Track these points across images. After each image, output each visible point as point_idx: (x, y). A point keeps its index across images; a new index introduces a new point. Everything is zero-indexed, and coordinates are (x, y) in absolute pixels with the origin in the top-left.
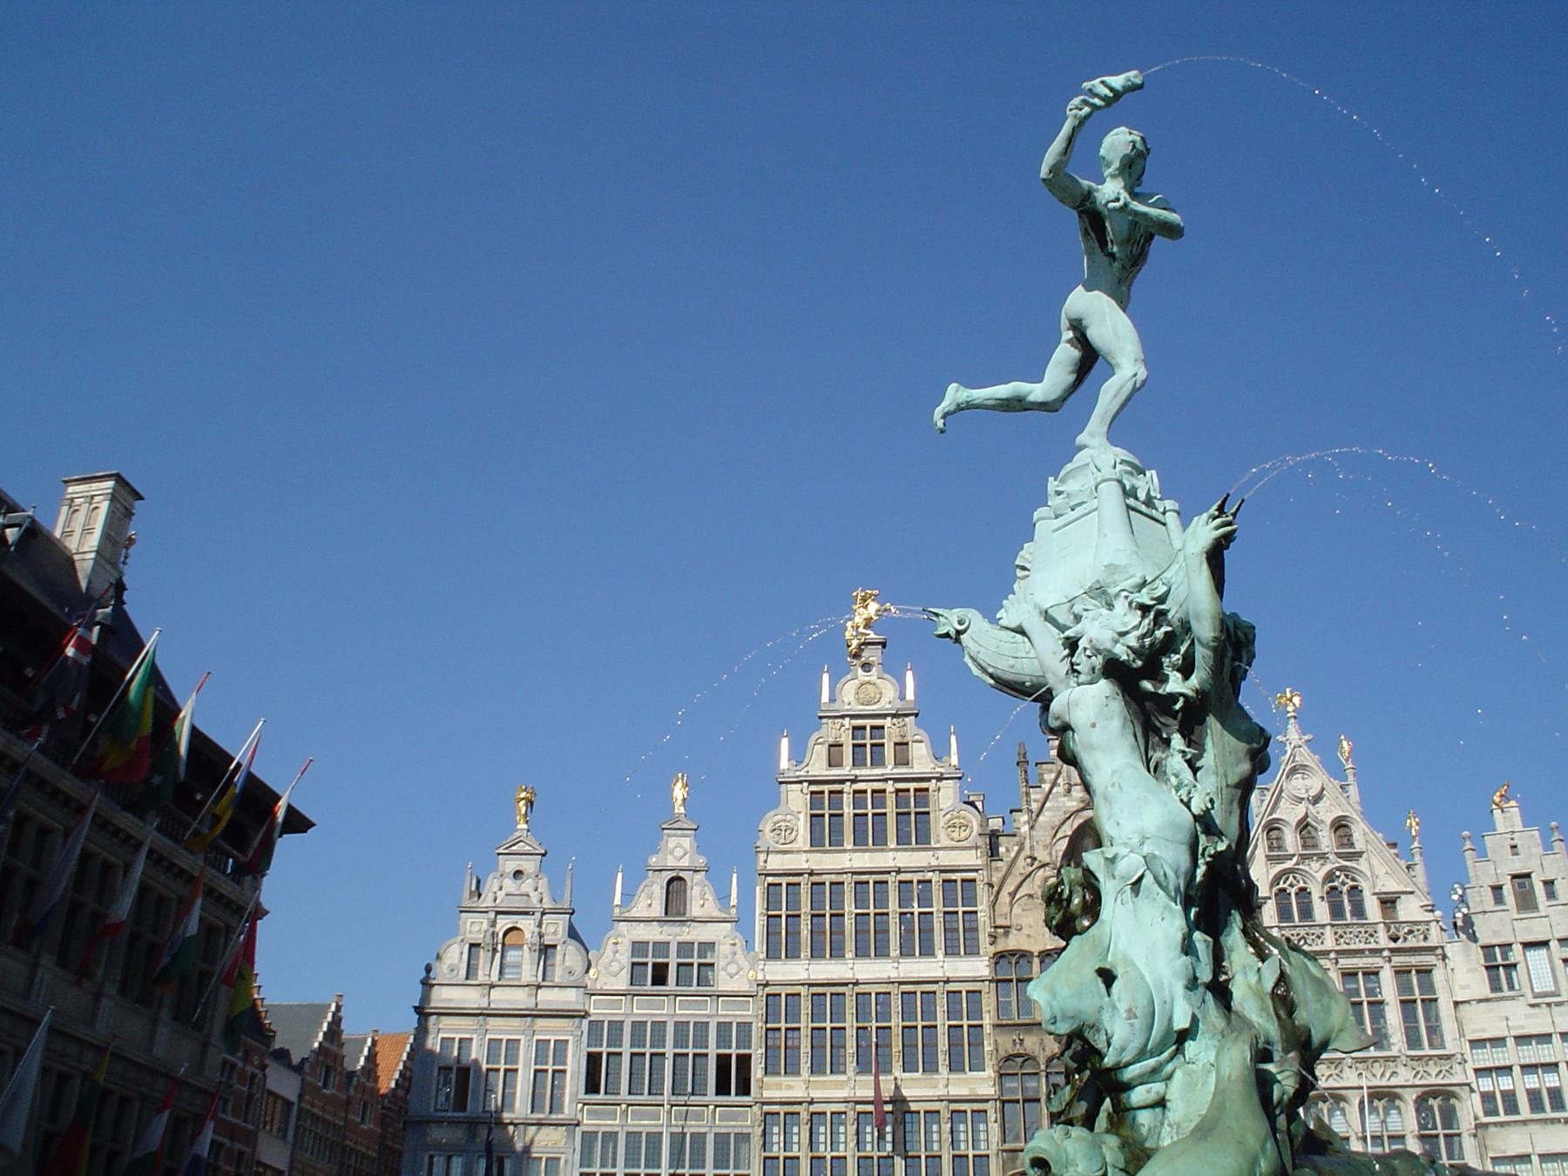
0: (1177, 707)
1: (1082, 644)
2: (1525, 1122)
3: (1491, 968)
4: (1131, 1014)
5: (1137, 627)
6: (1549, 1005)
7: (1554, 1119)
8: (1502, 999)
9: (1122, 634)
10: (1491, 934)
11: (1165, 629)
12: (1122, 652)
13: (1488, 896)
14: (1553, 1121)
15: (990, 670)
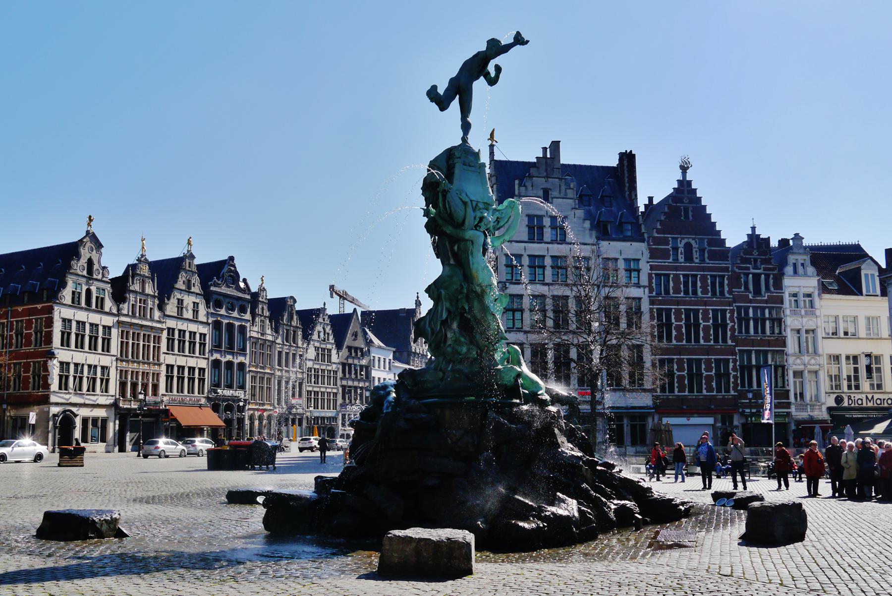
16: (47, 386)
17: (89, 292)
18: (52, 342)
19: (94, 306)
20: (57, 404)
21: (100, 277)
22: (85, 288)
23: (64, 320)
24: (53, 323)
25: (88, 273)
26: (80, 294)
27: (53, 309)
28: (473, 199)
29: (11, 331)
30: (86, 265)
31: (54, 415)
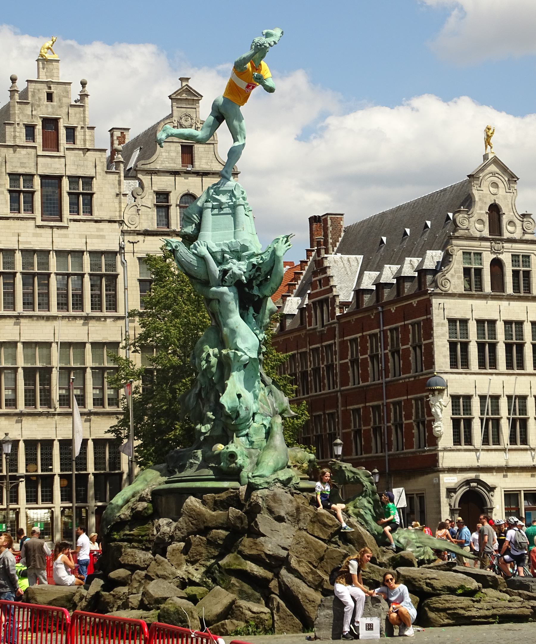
0: (256, 300)
1: (230, 272)
2: (18, 317)
3: (14, 194)
4: (247, 409)
5: (250, 271)
6: (52, 227)
7: (40, 316)
8: (18, 219)
9: (244, 272)
10: (19, 165)
11: (258, 273)
12: (244, 278)
13: (22, 132)
14: (40, 318)
15: (186, 269)
16: (433, 440)
17: (497, 264)
18: (433, 363)
19: (509, 289)
20: (452, 470)
21: (517, 235)
22: (488, 258)
23: (452, 321)
24: (432, 329)
25: (491, 232)
26: (479, 272)
27: (431, 305)
28: (215, 249)
29: (385, 349)
30: (486, 218)
31: (450, 491)
